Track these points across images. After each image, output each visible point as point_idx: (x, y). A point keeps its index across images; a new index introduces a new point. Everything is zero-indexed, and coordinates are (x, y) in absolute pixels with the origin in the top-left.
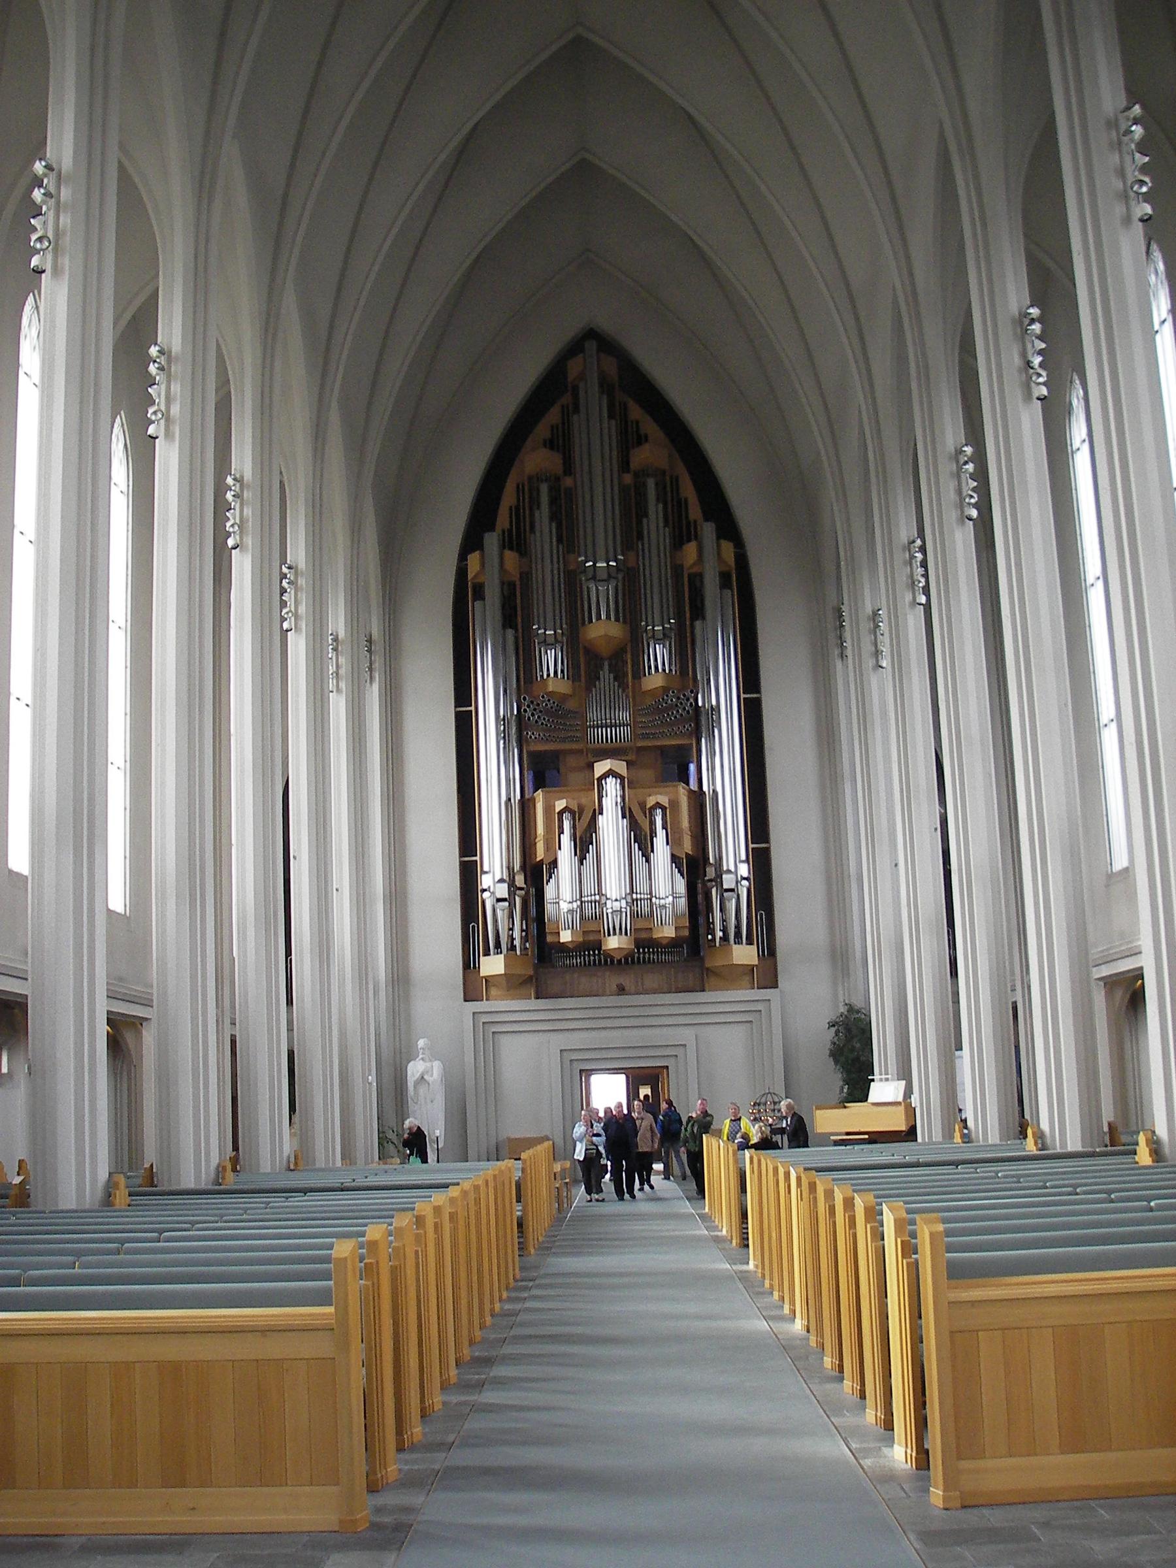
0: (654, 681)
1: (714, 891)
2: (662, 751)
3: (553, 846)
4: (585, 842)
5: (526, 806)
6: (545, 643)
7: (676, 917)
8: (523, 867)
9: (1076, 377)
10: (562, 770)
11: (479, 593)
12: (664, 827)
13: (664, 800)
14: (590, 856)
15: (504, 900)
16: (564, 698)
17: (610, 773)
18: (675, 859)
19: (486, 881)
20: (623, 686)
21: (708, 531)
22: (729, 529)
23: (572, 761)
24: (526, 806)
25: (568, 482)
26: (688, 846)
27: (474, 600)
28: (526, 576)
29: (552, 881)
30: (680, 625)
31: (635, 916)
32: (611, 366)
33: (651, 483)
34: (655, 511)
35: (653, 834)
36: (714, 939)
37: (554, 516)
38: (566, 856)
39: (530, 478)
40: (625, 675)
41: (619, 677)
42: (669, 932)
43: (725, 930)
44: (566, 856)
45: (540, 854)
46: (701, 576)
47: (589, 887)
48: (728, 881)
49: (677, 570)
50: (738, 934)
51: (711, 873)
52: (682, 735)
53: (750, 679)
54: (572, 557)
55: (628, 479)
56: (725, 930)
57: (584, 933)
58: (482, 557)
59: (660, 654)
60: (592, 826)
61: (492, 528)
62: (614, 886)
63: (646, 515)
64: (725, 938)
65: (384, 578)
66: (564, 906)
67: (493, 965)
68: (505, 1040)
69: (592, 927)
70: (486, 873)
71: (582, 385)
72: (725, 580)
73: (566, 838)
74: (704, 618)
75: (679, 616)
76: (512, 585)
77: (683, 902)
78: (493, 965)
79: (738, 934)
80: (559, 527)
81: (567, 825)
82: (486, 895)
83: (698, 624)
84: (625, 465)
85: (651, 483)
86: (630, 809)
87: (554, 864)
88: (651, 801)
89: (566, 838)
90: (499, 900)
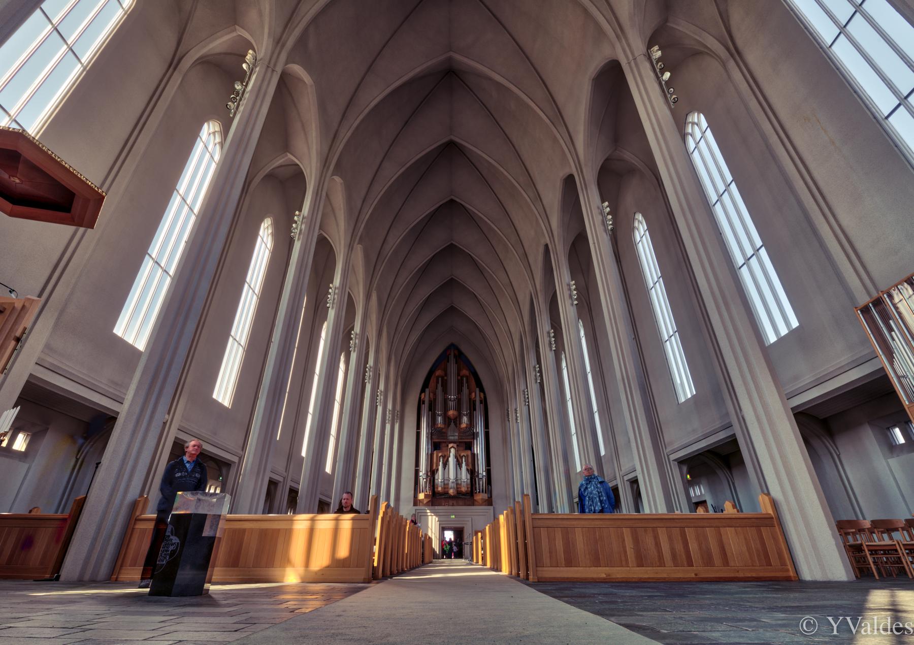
0: (463, 425)
1: (477, 479)
2: (465, 442)
3: (438, 465)
4: (445, 464)
5: (432, 455)
6: (438, 415)
7: (467, 484)
8: (430, 471)
9: (563, 352)
10: (441, 446)
11: (424, 403)
12: (465, 461)
13: (465, 455)
14: (447, 468)
16: (443, 429)
17: (452, 447)
18: (467, 469)
19: (421, 474)
20: (457, 427)
21: (477, 390)
22: (482, 390)
23: (444, 445)
24: (432, 455)
25: (446, 378)
26: (470, 467)
27: (423, 404)
28: (435, 400)
29: (437, 474)
30: (470, 412)
31: (457, 484)
32: (456, 352)
33: (465, 379)
34: (465, 385)
35: (462, 463)
36: (477, 492)
37: (442, 386)
38: (440, 468)
39: (437, 377)
40: (457, 424)
41: (456, 425)
42: (464, 489)
43: (479, 490)
44: (440, 468)
45: (434, 467)
46: (476, 401)
47: (446, 476)
48: (480, 476)
49: (470, 399)
50: (483, 491)
51: (476, 474)
52: (470, 439)
53: (487, 426)
54: (445, 395)
55: (459, 378)
56: (479, 490)
57: (445, 488)
58: (425, 394)
59: (465, 419)
60: (447, 460)
61: (428, 388)
62: (452, 476)
63: (463, 386)
64: (479, 492)
66: (440, 480)
67: (421, 496)
71: (450, 356)
72: (481, 402)
73: (441, 463)
75: (470, 410)
76: (431, 401)
77: (469, 481)
78: (421, 496)
79: (483, 491)
80: (443, 389)
81: (441, 460)
82: (421, 477)
83: (475, 412)
84: (459, 374)
85: (465, 379)
87: (438, 470)
88: (462, 455)
89: (441, 463)
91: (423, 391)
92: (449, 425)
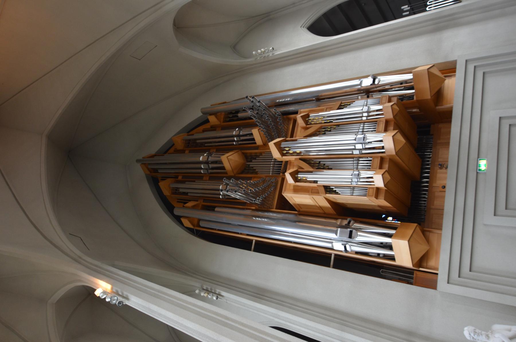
14: (328, 163)
15: (351, 232)
29: (338, 190)
57: (381, 168)
65: (186, 274)
68: (480, 262)
69: (377, 162)
70: (332, 245)
74: (237, 112)
86: (304, 137)
87: (328, 189)
90: (350, 236)
91: (178, 219)
92: (254, 172)
